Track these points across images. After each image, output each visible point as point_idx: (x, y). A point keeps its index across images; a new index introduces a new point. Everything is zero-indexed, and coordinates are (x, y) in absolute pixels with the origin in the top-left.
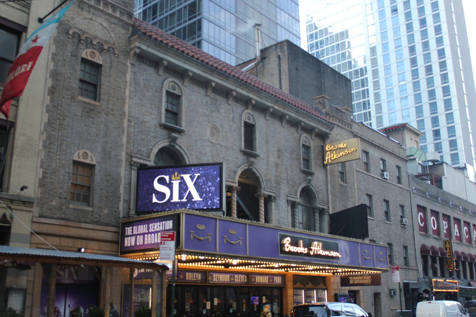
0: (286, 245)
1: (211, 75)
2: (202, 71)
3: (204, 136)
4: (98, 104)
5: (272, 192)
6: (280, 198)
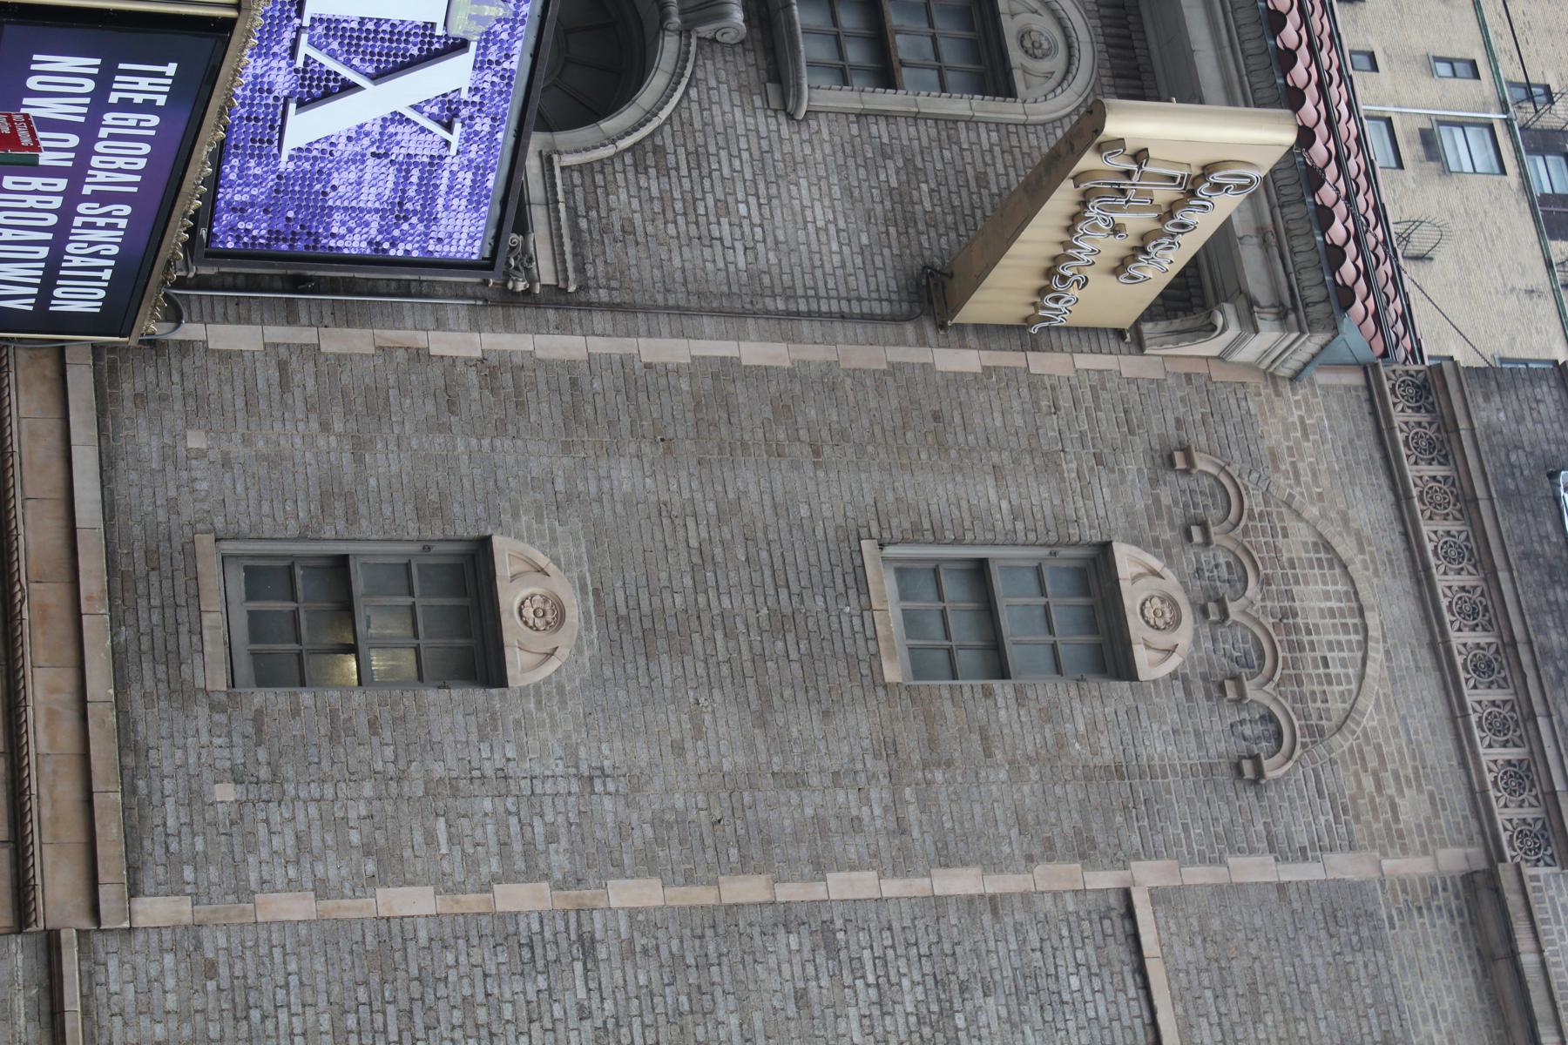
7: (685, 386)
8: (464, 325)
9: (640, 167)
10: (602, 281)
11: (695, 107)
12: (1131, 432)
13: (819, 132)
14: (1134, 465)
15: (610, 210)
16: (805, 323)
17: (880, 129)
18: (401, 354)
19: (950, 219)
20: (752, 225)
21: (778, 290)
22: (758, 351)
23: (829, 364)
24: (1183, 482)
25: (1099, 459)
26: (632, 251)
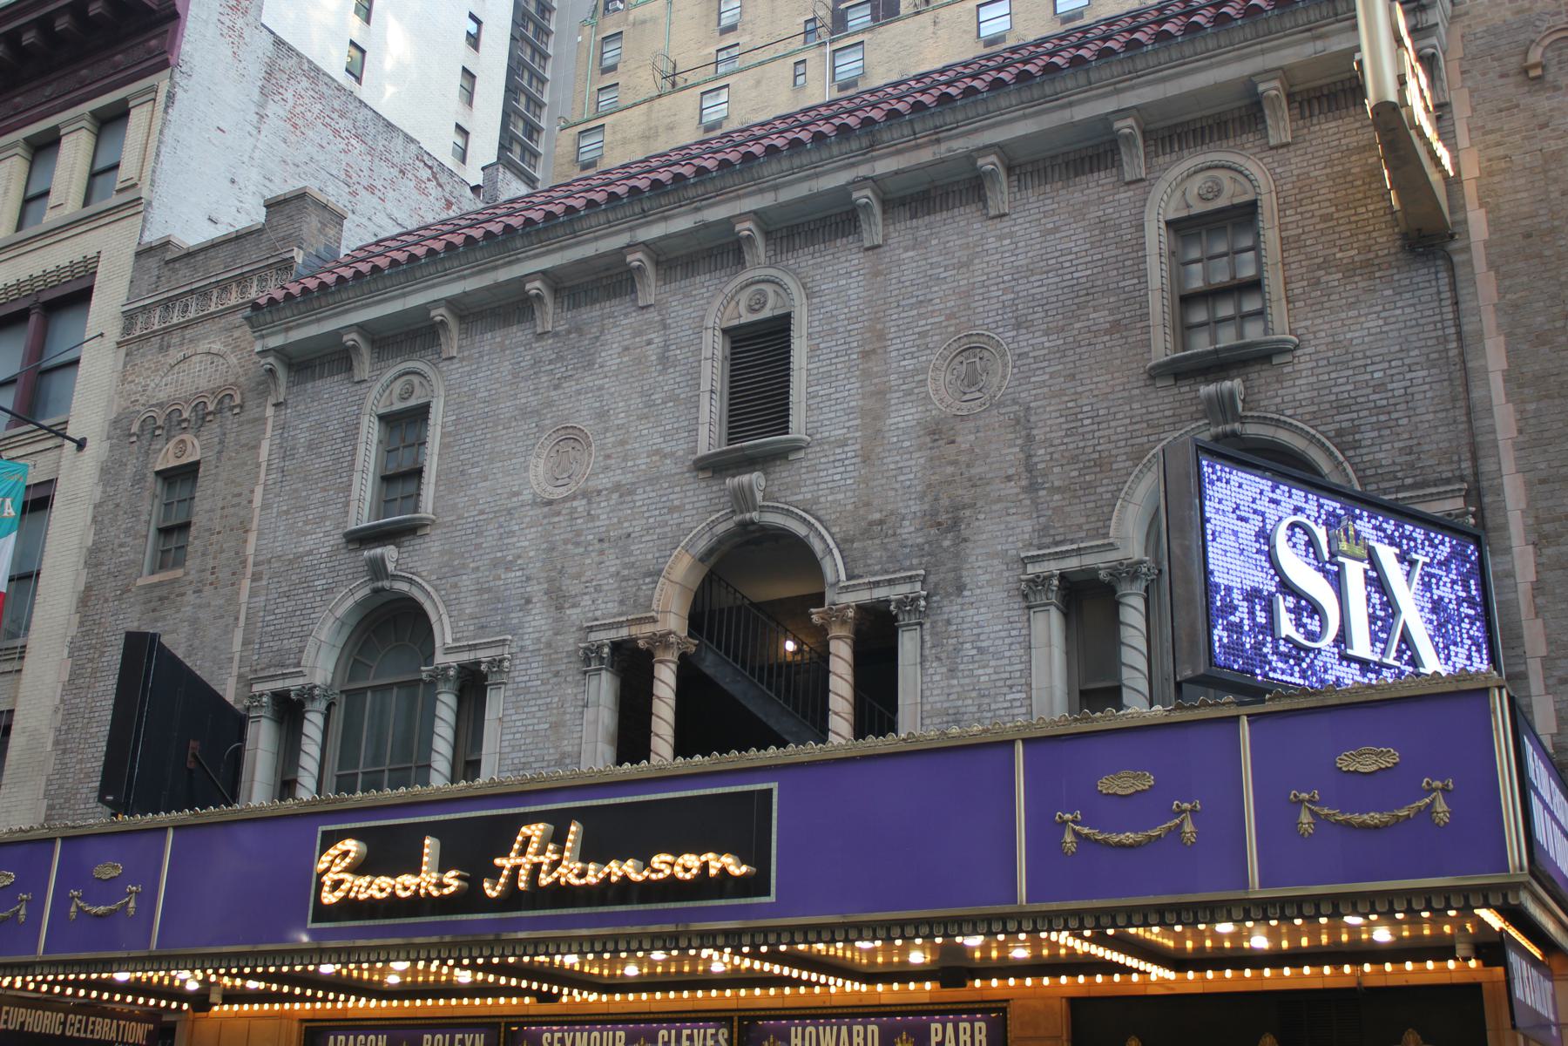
0: (327, 880)
1: (510, 263)
2: (473, 275)
3: (517, 494)
4: (179, 573)
5: (891, 582)
6: (960, 588)
7: (1533, 406)
8: (1508, 558)
9: (1356, 445)
10: (1455, 466)
11: (1299, 411)
12: (1517, 106)
13: (1306, 328)
14: (1543, 103)
15: (1394, 463)
16: (1465, 328)
17: (1297, 287)
18: (1539, 600)
19: (1361, 237)
20: (1390, 368)
21: (1441, 347)
22: (1494, 357)
23: (1497, 308)
24: (1553, 70)
25: (1545, 125)
26: (1426, 447)
